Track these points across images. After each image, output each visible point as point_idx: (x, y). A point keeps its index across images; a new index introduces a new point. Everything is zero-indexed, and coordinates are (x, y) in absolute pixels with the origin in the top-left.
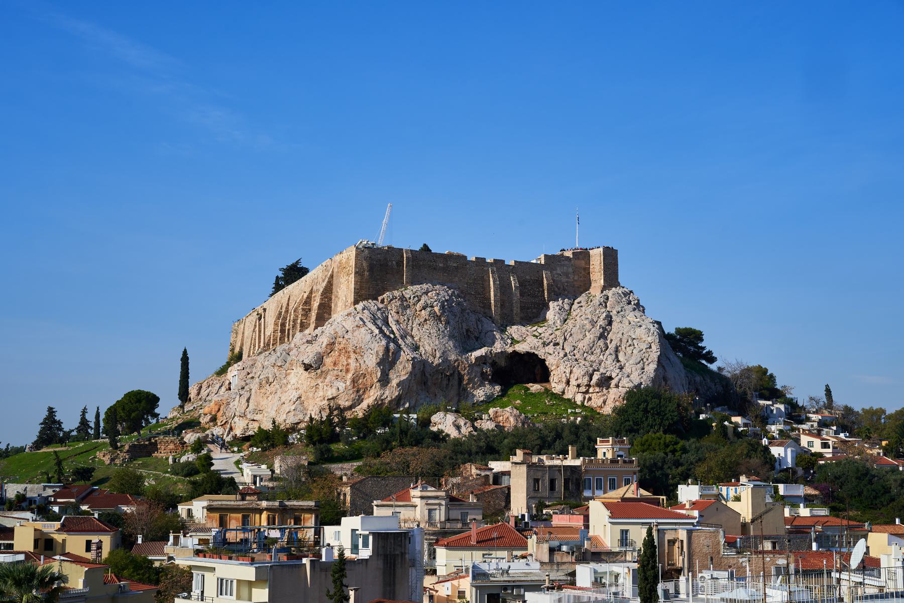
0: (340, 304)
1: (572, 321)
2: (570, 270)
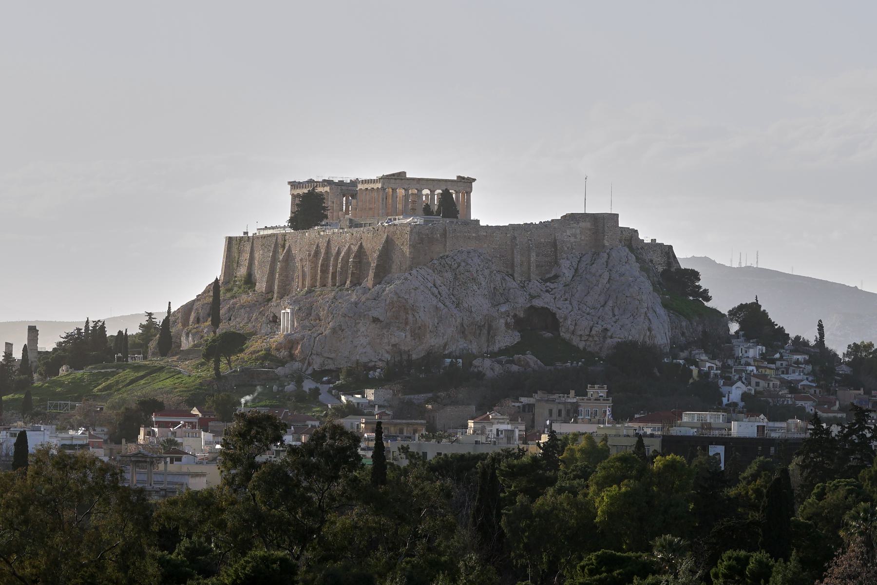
0: (394, 267)
1: (578, 278)
2: (578, 231)
